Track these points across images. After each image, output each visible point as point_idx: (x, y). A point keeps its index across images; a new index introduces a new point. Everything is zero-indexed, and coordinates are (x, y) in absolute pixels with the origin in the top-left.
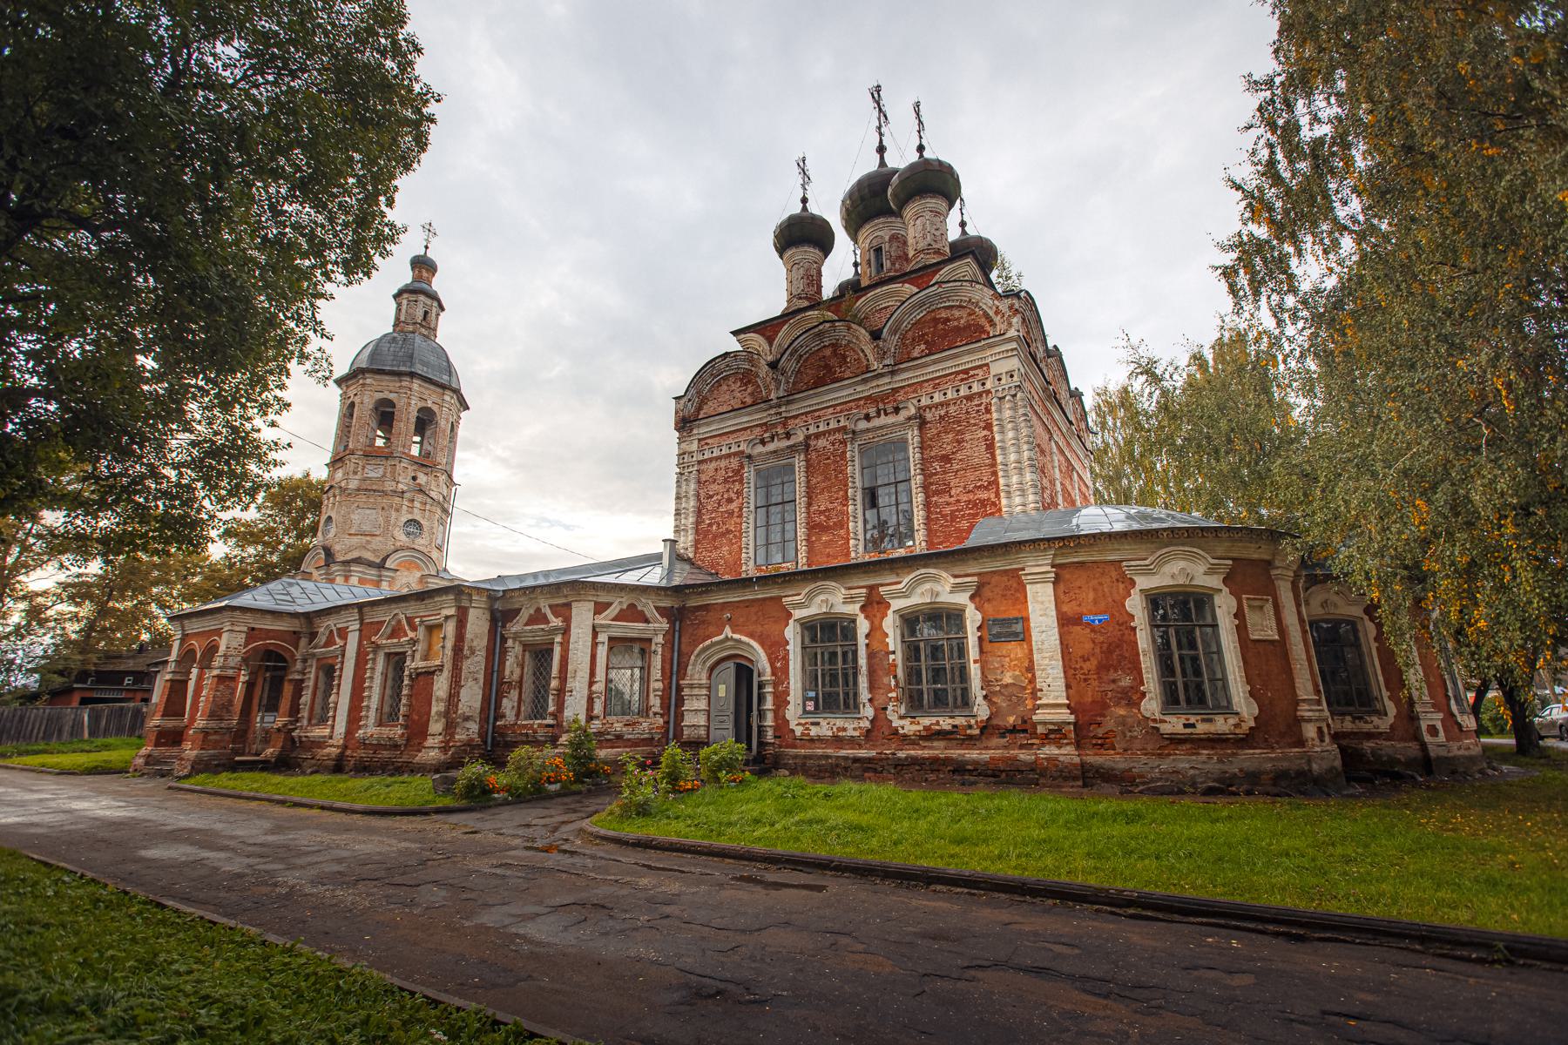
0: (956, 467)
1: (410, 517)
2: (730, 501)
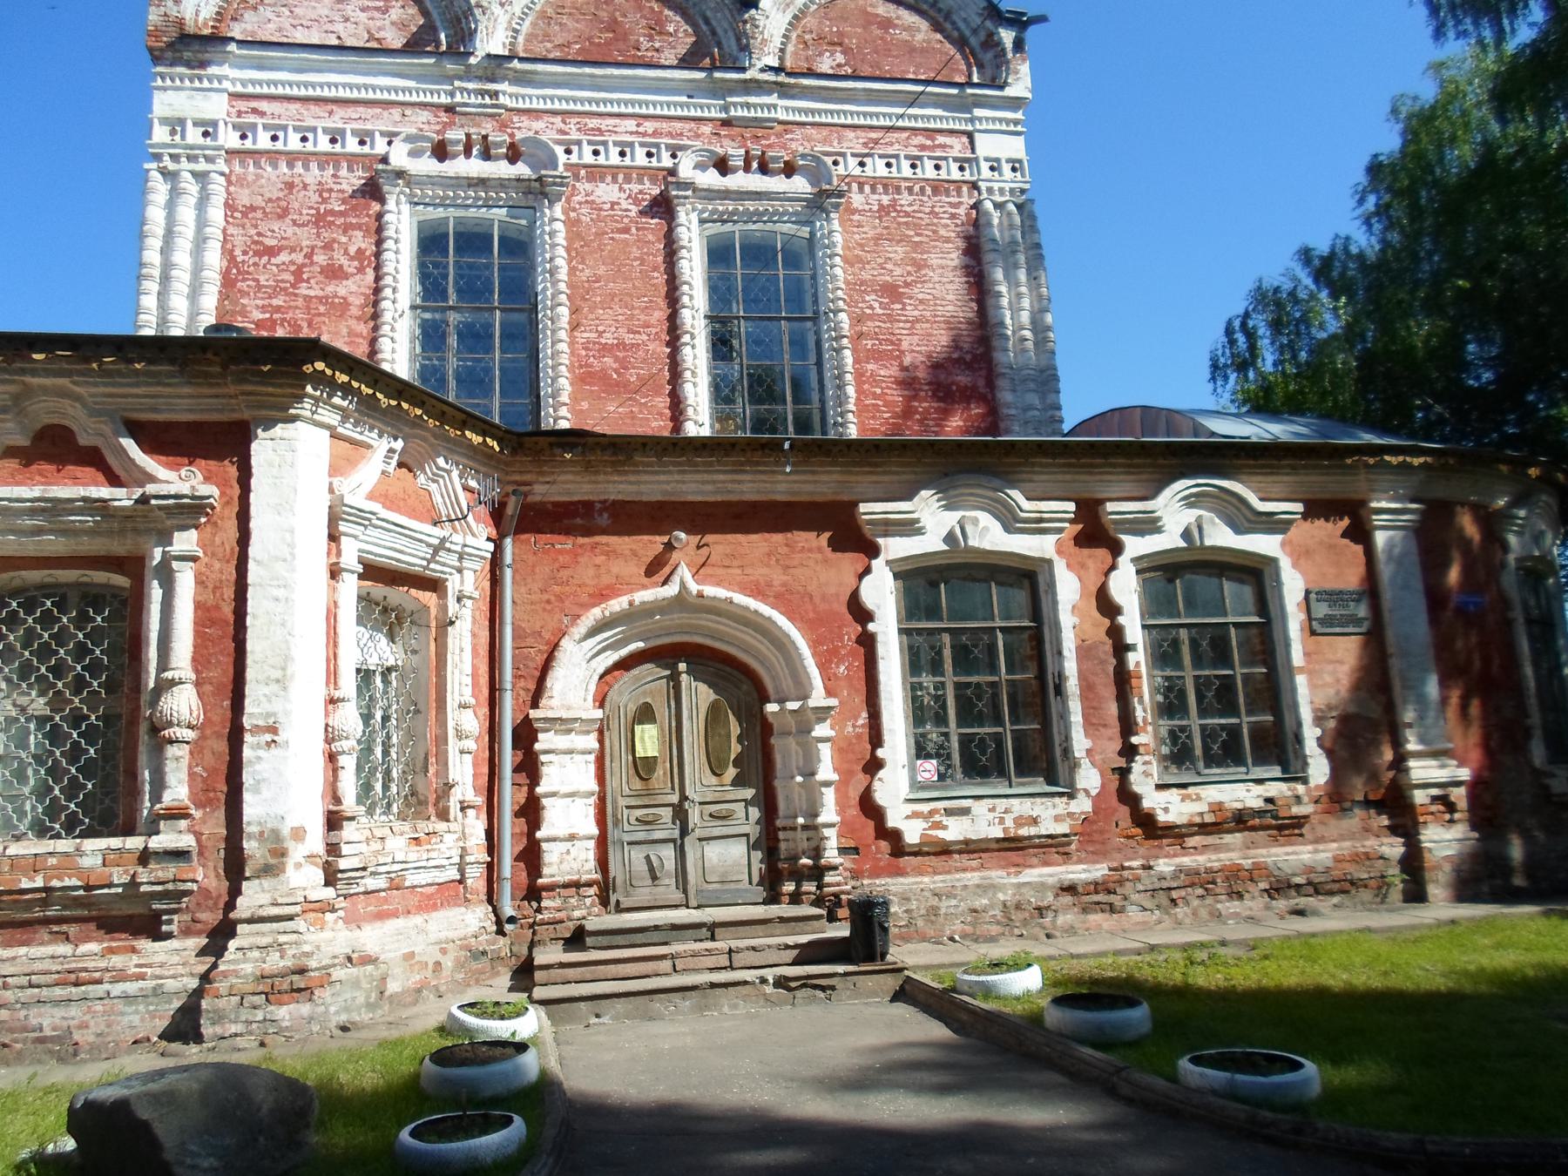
0: (912, 312)
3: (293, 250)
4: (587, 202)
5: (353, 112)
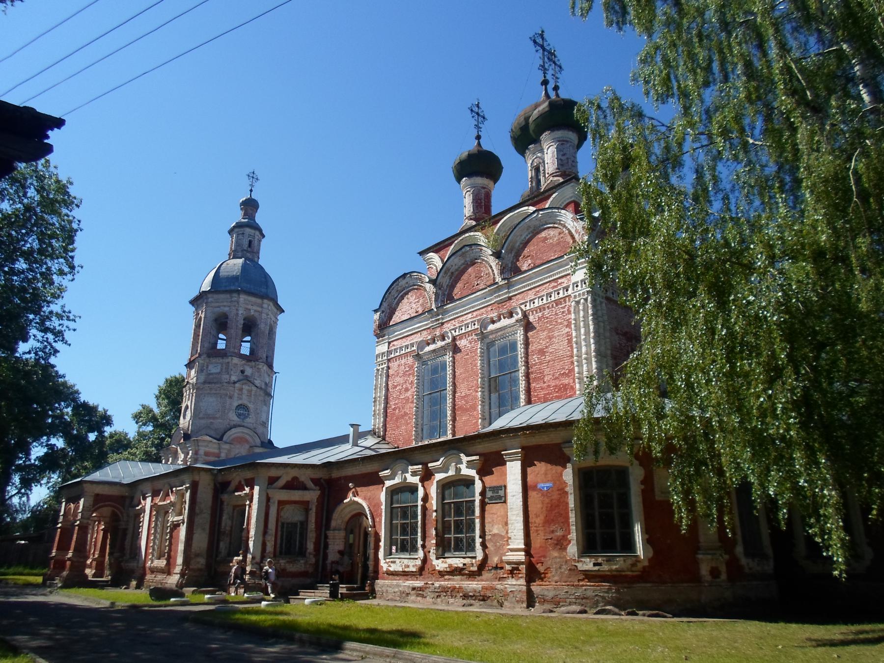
0: (548, 358)
1: (240, 402)
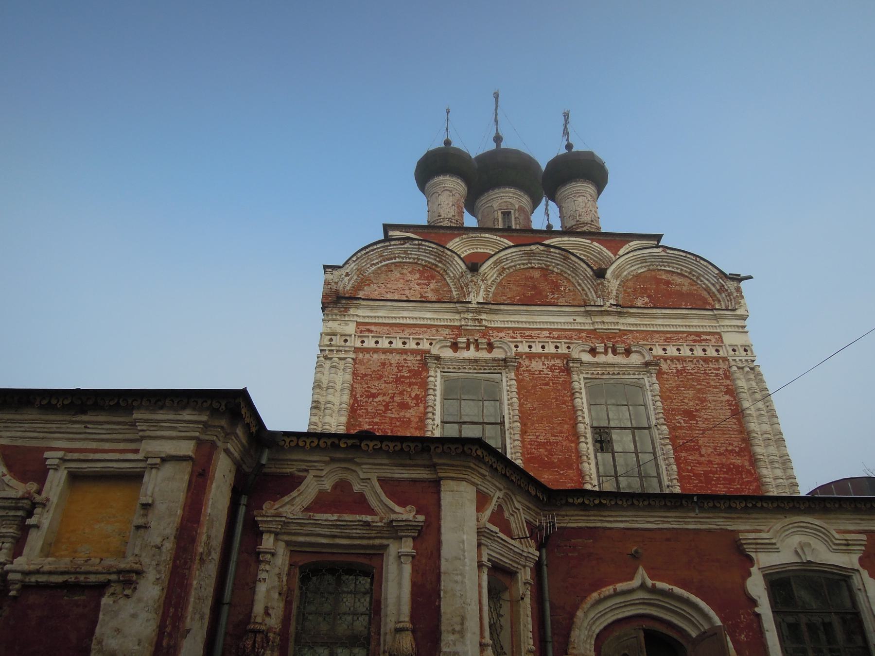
2: (404, 406)
3: (384, 395)
4: (527, 370)
5: (412, 330)
